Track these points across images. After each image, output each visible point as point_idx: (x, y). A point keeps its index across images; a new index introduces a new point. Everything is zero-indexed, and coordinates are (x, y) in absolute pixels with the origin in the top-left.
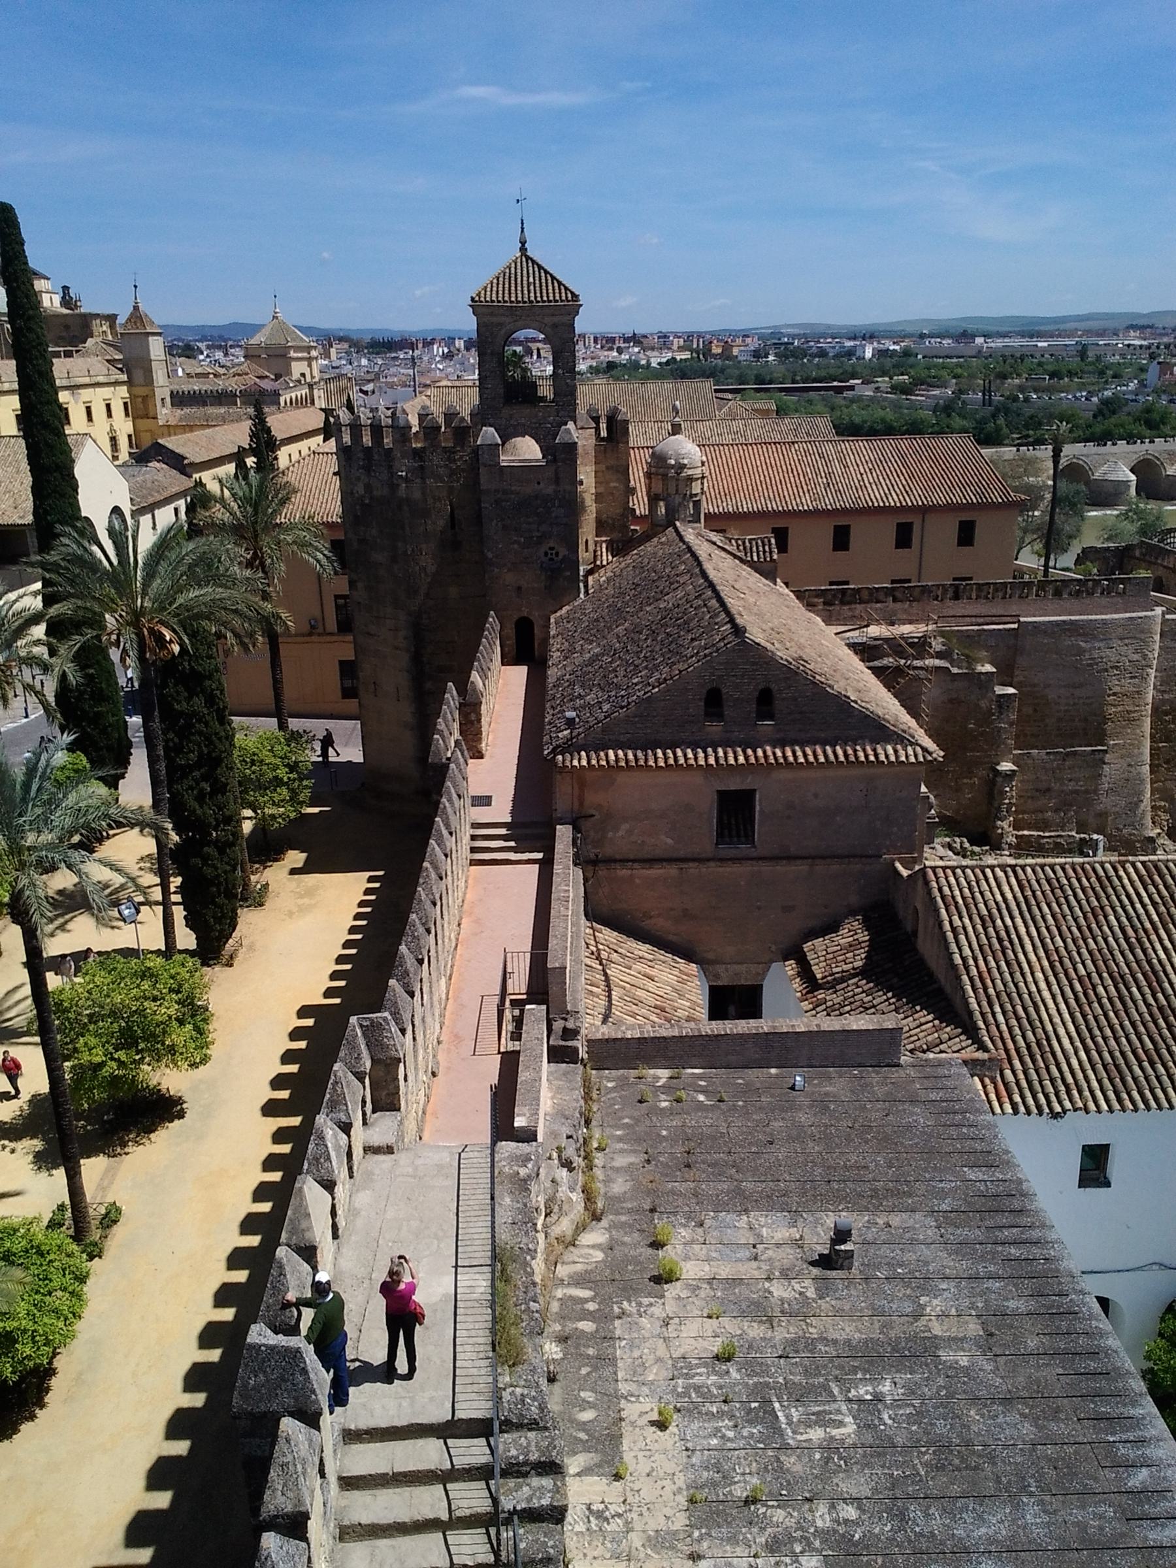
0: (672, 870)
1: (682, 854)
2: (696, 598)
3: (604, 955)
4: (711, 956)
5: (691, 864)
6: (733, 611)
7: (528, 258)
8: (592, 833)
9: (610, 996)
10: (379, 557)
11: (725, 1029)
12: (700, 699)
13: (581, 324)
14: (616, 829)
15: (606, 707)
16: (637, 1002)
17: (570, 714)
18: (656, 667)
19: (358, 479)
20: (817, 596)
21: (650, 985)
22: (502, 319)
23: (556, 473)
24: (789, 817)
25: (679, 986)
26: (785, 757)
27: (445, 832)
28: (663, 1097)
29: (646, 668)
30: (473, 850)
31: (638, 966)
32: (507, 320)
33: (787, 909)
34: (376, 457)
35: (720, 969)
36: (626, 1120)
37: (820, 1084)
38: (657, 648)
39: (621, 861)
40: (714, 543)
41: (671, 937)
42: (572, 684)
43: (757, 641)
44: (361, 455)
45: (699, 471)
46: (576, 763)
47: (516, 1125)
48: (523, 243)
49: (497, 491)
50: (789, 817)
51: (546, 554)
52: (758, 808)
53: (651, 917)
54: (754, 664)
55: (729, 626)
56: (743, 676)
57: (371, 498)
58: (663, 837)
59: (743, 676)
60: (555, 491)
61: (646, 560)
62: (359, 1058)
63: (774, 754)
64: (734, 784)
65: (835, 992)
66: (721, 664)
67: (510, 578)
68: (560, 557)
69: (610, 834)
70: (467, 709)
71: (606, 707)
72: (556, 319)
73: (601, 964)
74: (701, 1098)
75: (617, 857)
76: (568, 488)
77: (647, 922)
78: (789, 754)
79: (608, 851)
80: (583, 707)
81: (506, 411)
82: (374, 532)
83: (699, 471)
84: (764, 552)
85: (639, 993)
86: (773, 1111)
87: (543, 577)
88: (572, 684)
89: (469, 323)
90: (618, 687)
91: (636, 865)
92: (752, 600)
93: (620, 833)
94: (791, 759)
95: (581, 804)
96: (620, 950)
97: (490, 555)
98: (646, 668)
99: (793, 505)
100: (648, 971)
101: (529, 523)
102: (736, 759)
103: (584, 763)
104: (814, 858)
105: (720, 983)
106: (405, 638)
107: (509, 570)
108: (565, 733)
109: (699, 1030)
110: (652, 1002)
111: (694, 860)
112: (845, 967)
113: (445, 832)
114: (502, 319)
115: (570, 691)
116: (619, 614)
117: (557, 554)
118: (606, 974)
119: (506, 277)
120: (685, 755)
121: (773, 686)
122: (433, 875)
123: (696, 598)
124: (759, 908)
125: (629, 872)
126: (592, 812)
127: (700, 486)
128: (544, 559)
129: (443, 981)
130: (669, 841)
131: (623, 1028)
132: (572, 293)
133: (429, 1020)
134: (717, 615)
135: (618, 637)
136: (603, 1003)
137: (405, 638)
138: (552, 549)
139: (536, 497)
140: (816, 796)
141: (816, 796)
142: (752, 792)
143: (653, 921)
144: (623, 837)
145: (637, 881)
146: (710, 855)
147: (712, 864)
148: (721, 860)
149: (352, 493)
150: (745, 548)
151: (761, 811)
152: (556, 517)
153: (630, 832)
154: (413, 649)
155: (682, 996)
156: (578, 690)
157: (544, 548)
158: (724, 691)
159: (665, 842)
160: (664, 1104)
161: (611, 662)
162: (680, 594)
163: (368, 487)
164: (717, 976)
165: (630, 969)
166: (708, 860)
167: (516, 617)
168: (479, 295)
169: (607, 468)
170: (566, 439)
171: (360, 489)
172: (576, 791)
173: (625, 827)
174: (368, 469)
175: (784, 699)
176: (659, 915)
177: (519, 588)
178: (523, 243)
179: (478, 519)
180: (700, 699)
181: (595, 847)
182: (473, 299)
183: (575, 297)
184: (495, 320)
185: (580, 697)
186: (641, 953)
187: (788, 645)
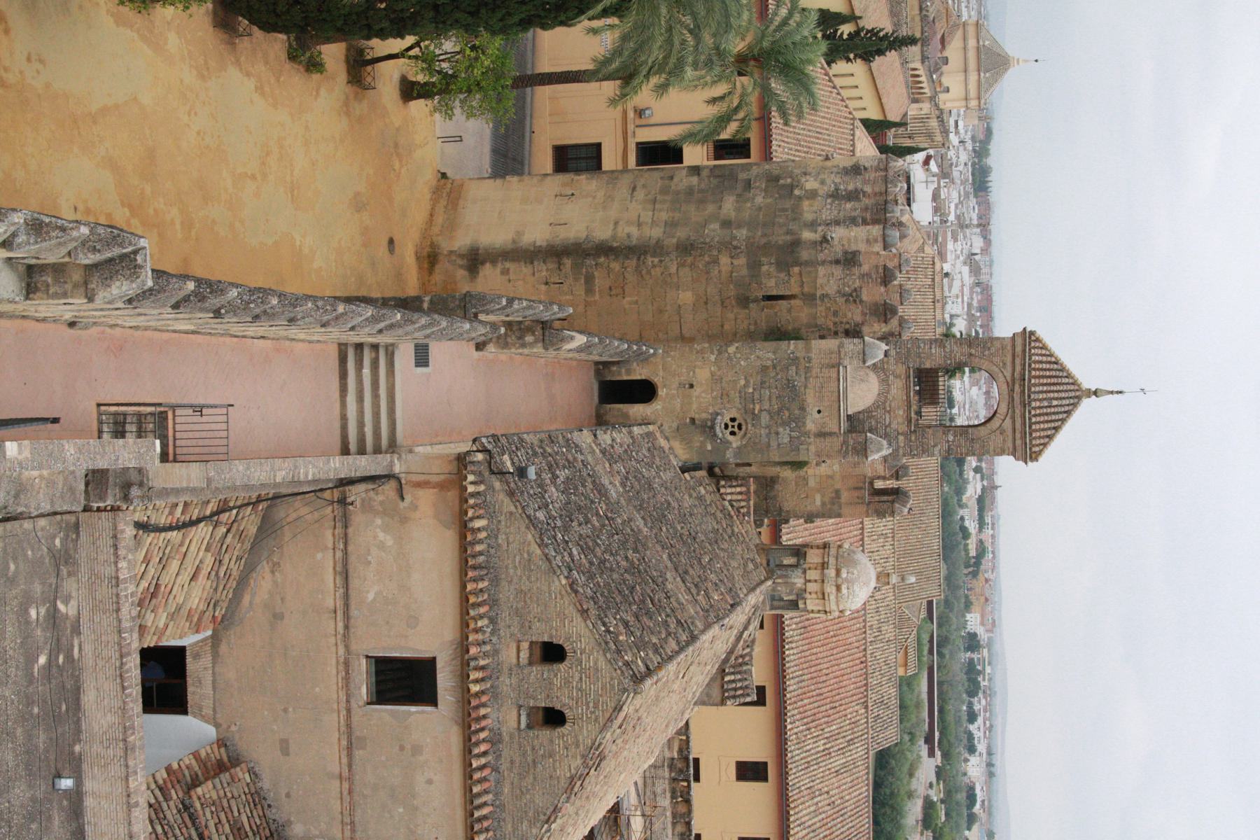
0: (330, 599)
1: (354, 612)
2: (679, 622)
3: (224, 517)
4: (223, 648)
5: (341, 625)
6: (662, 673)
7: (1079, 398)
8: (380, 498)
9: (170, 528)
10: (729, 205)
11: (130, 686)
12: (551, 637)
13: (1006, 466)
14: (386, 529)
15: (541, 515)
16: (163, 564)
17: (532, 473)
18: (591, 577)
19: (823, 182)
20: (680, 751)
21: (185, 577)
23: (831, 434)
24: (402, 748)
25: (184, 612)
26: (477, 744)
27: (382, 325)
28: (43, 611)
29: (591, 563)
30: (359, 347)
31: (209, 560)
33: (285, 747)
34: (849, 206)
35: (207, 660)
36: (12, 567)
37: (61, 808)
38: (615, 576)
39: (346, 535)
40: (746, 628)
41: (246, 599)
42: (570, 464)
43: (625, 708)
44: (851, 187)
45: (834, 607)
46: (471, 478)
47: (8, 444)
48: (1096, 393)
50: (402, 748)
51: (733, 420)
52: (413, 709)
53: (273, 572)
54: (596, 706)
55: (642, 668)
56: (580, 690)
57: (800, 198)
58: (376, 588)
59: (580, 690)
60: (807, 434)
61: (725, 546)
62: (94, 250)
63: (483, 729)
64: (445, 680)
65: (179, 811)
66: (596, 663)
67: (703, 374)
68: (731, 438)
69: (379, 521)
70: (538, 332)
71: (541, 515)
73: (213, 514)
74: (42, 660)
75: (350, 530)
77: (267, 569)
78: (483, 748)
79: (358, 518)
80: (541, 486)
81: (901, 369)
82: (759, 200)
83: (834, 607)
84: (735, 689)
85: (175, 565)
86: (27, 752)
87: (704, 416)
88: (570, 464)
89: (1005, 327)
90: (566, 529)
91: (339, 554)
92: (675, 687)
93: (381, 536)
94: (476, 751)
95: (419, 485)
96: (230, 536)
97: (731, 349)
98: (591, 563)
99: (792, 711)
100: (204, 572)
101: (770, 399)
102: (477, 681)
103: (471, 489)
104: (350, 780)
105: (189, 660)
106: (629, 236)
107: (713, 374)
108: (509, 464)
109: (129, 654)
110: (163, 582)
111: (347, 627)
112: (211, 824)
113: (382, 325)
115: (561, 463)
116: (658, 518)
117: (733, 433)
118: (199, 521)
119: (1058, 373)
120: (481, 617)
121: (568, 726)
122: (325, 318)
123: (679, 622)
124: (285, 710)
125: (330, 545)
126: (408, 498)
127: (815, 608)
128: (727, 419)
129: (192, 328)
130: (371, 596)
131: (130, 557)
132: (1040, 452)
133: (142, 318)
134: (656, 651)
135: (630, 520)
136: (163, 520)
137: (629, 236)
138: (740, 427)
139: (802, 409)
140: (430, 782)
141: (430, 782)
142: (434, 702)
143: (268, 576)
144: (375, 537)
145: (319, 556)
146: (354, 647)
147: (341, 651)
148: (347, 664)
149: (805, 174)
150: (741, 665)
151: (410, 714)
152: (777, 433)
153: (382, 546)
154: (615, 245)
155: (172, 617)
156: (562, 474)
158: (562, 666)
159: (369, 589)
160: (33, 613)
161: (597, 514)
162: (684, 597)
163: (813, 194)
164: (197, 656)
165: (207, 550)
166: (347, 647)
167: (657, 380)
168: (1038, 340)
169: (837, 492)
170: (871, 447)
171: (811, 184)
172: (434, 479)
173: (390, 542)
174: (835, 195)
175: (552, 741)
176: (275, 583)
178: (1096, 393)
179: (778, 334)
180: (551, 637)
181: (363, 500)
182: (1032, 333)
183: (1034, 457)
185: (555, 477)
186: (226, 561)
187: (619, 741)
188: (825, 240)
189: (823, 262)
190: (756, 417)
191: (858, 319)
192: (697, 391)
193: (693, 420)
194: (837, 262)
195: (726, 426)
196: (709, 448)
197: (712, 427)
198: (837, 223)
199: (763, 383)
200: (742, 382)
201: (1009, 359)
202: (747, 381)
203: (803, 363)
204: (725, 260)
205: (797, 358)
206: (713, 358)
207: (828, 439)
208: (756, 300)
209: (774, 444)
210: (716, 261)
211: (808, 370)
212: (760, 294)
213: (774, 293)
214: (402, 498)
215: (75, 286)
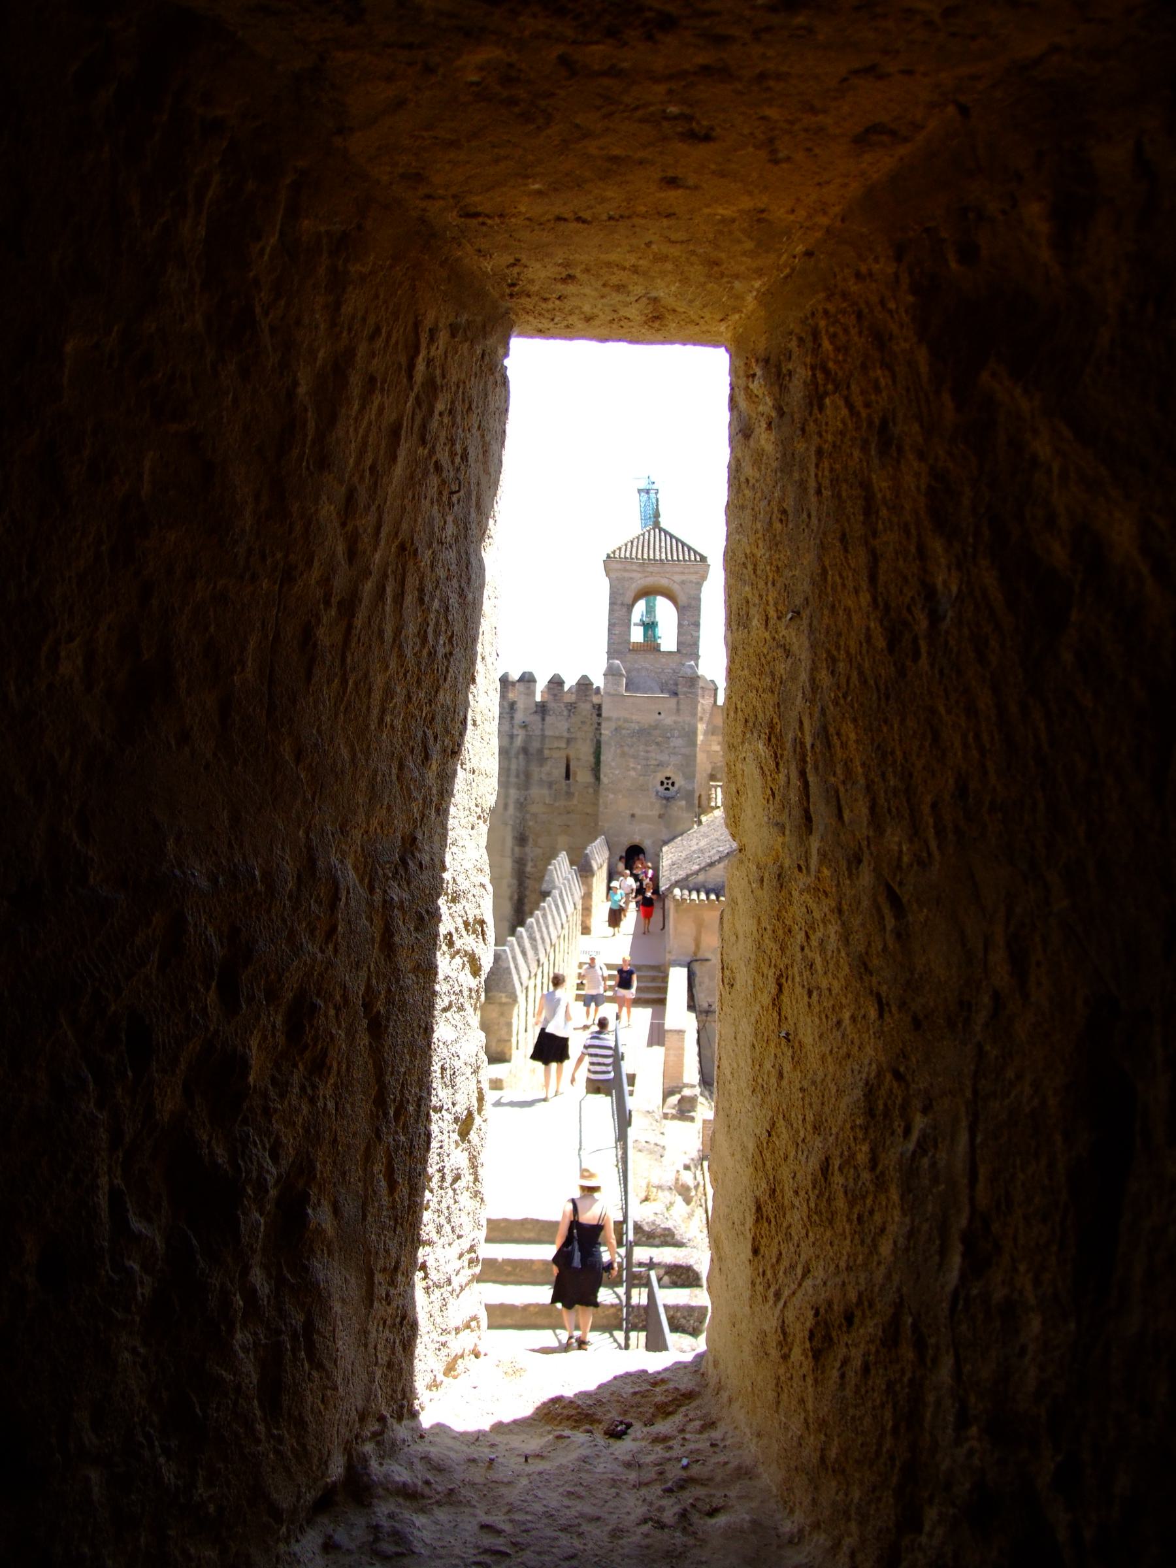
7: (661, 530)
8: (706, 980)
22: (634, 575)
32: (639, 575)
49: (619, 719)
51: (662, 783)
68: (677, 785)
72: (684, 578)
76: (688, 719)
87: (657, 806)
95: (698, 946)
114: (634, 575)
117: (673, 784)
137: (509, 886)
138: (668, 778)
139: (656, 727)
154: (516, 897)
157: (660, 777)
168: (614, 552)
177: (633, 816)
182: (608, 556)
184: (626, 575)
188: (525, 726)
189: (543, 730)
190: (660, 765)
191: (588, 706)
192: (637, 811)
193: (660, 816)
194: (543, 719)
195: (667, 789)
196: (684, 803)
197: (667, 799)
198: (512, 718)
199: (634, 757)
200: (633, 773)
201: (626, 575)
202: (634, 769)
203: (620, 723)
204: (534, 809)
205: (616, 729)
206: (611, 796)
207: (681, 707)
208: (568, 786)
209: (683, 751)
210: (535, 815)
211: (626, 721)
212: (564, 782)
213: (564, 771)
214: (707, 960)
215: (502, 1014)
